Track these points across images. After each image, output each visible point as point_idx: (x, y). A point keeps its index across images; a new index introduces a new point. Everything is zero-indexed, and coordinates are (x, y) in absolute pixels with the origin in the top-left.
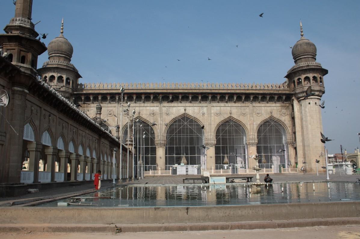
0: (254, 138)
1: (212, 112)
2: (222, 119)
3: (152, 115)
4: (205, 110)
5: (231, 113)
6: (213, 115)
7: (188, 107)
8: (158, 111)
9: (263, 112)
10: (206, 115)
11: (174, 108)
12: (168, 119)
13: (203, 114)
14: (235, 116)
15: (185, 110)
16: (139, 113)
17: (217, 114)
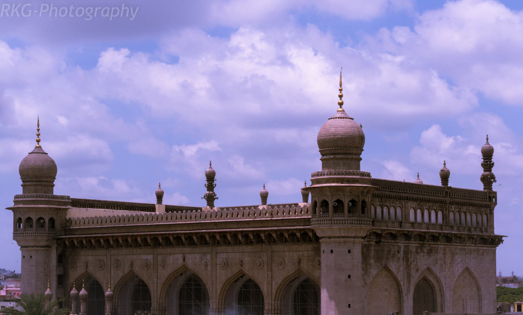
0: (270, 309)
1: (218, 262)
2: (229, 275)
3: (146, 269)
4: (209, 257)
5: (242, 265)
6: (218, 266)
7: (188, 255)
8: (152, 261)
9: (287, 261)
10: (209, 268)
11: (171, 258)
12: (165, 273)
13: (206, 266)
14: (247, 269)
15: (184, 260)
16: (132, 264)
17: (226, 265)
